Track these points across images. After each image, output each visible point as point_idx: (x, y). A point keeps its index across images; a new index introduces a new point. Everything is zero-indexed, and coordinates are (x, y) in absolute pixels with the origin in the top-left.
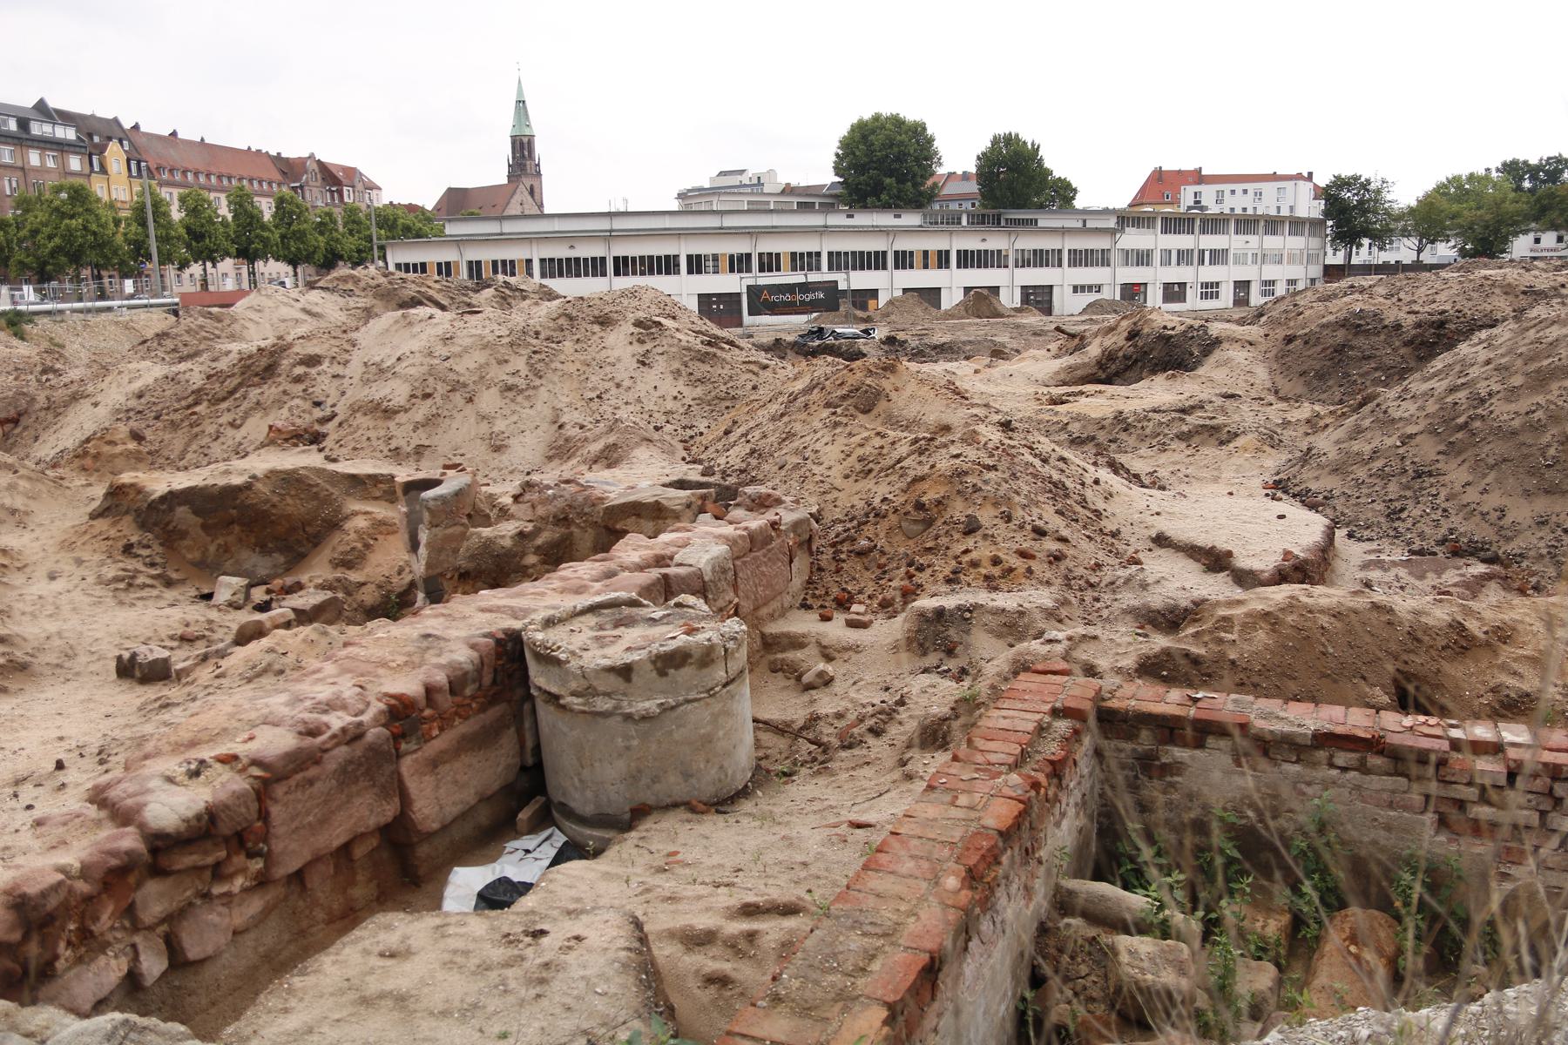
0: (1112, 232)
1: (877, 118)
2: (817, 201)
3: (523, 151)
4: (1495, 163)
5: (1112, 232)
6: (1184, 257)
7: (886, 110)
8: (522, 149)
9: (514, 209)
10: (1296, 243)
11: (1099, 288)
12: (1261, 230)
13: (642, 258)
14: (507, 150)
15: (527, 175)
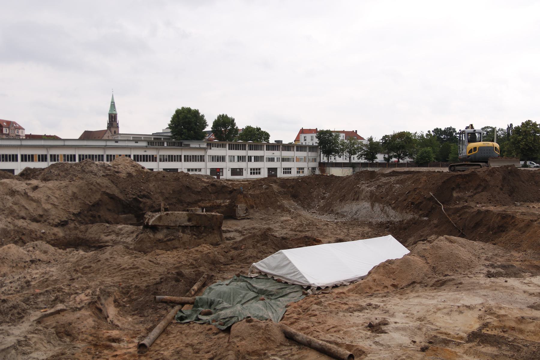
0: (205, 149)
1: (183, 108)
2: (162, 137)
3: (113, 119)
4: (432, 129)
5: (205, 149)
6: (241, 159)
7: (186, 106)
8: (113, 119)
9: (105, 137)
10: (312, 155)
11: (200, 170)
12: (281, 149)
14: (107, 119)
15: (113, 127)
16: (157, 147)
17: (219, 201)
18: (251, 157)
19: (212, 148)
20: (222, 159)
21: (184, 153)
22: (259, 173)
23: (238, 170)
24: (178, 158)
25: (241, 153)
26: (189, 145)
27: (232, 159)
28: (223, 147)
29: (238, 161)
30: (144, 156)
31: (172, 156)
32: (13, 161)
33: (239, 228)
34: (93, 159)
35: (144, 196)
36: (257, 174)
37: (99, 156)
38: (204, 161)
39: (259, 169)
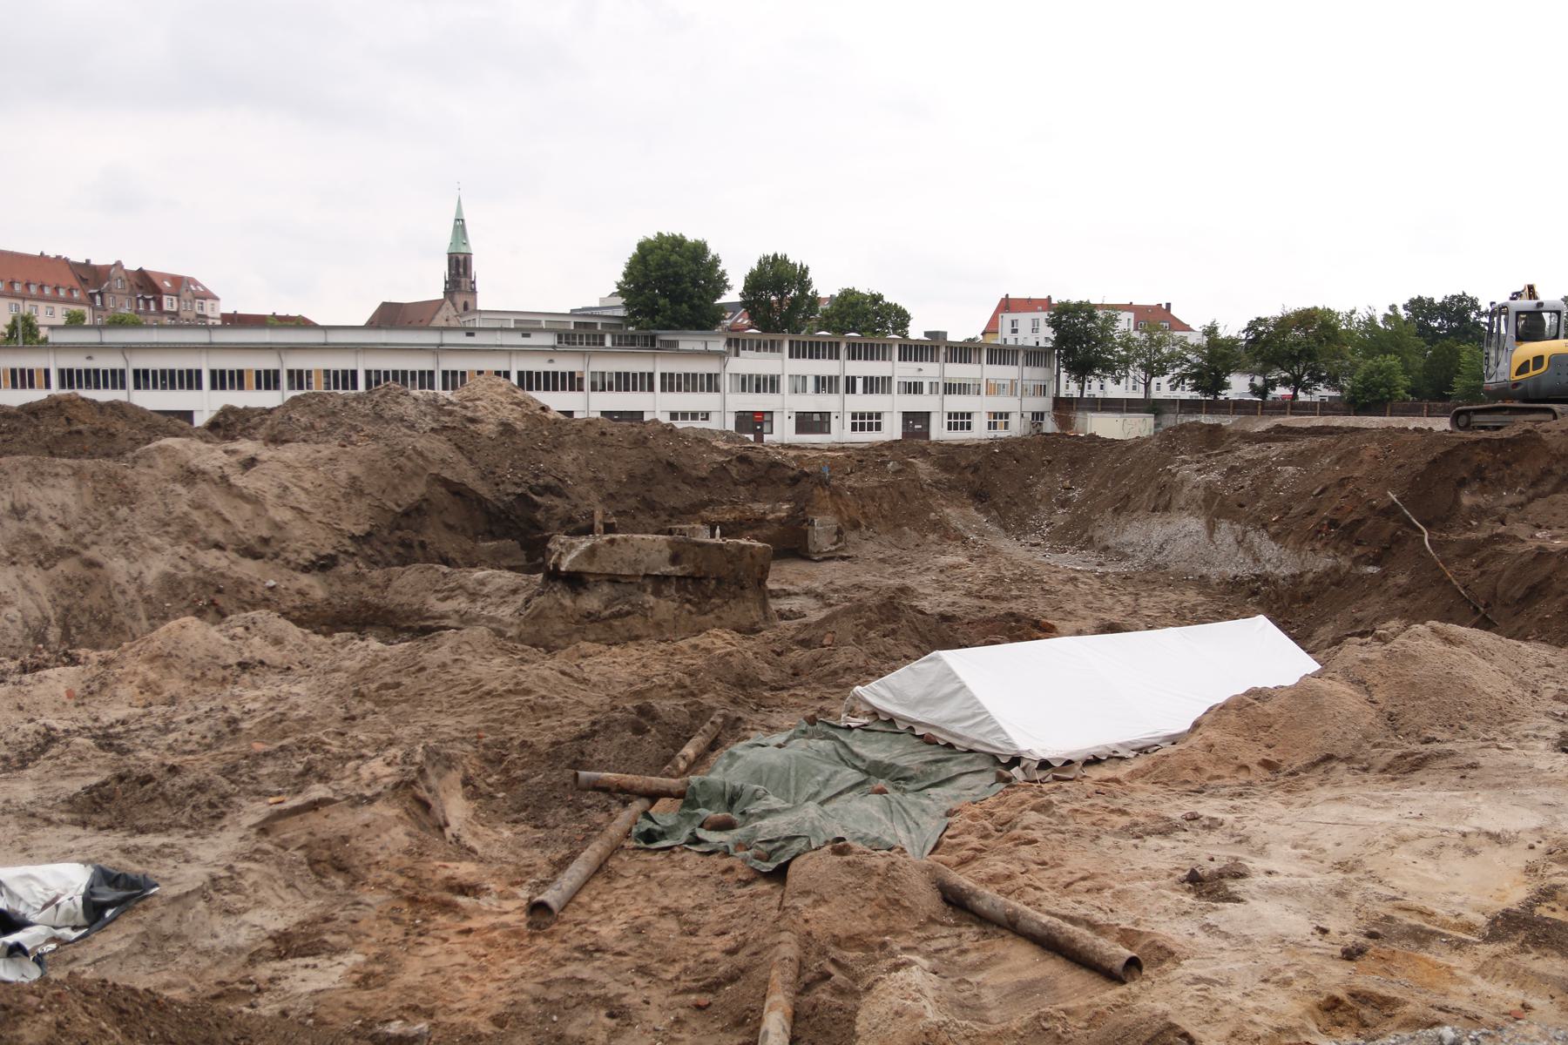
0: (721, 355)
2: (599, 321)
3: (459, 268)
4: (1401, 300)
5: (721, 355)
6: (824, 384)
8: (459, 268)
9: (439, 321)
10: (1035, 374)
11: (706, 416)
12: (942, 357)
13: (163, 372)
14: (441, 269)
15: (460, 291)
16: (584, 348)
17: (759, 508)
18: (854, 378)
19: (742, 353)
20: (769, 384)
21: (660, 366)
22: (878, 427)
23: (817, 418)
24: (643, 382)
25: (826, 367)
26: (674, 344)
27: (799, 385)
28: (773, 350)
29: (817, 391)
30: (546, 373)
31: (627, 374)
32: (190, 387)
33: (817, 586)
34: (404, 383)
35: (548, 489)
36: (870, 429)
37: (422, 373)
38: (717, 390)
39: (879, 415)
